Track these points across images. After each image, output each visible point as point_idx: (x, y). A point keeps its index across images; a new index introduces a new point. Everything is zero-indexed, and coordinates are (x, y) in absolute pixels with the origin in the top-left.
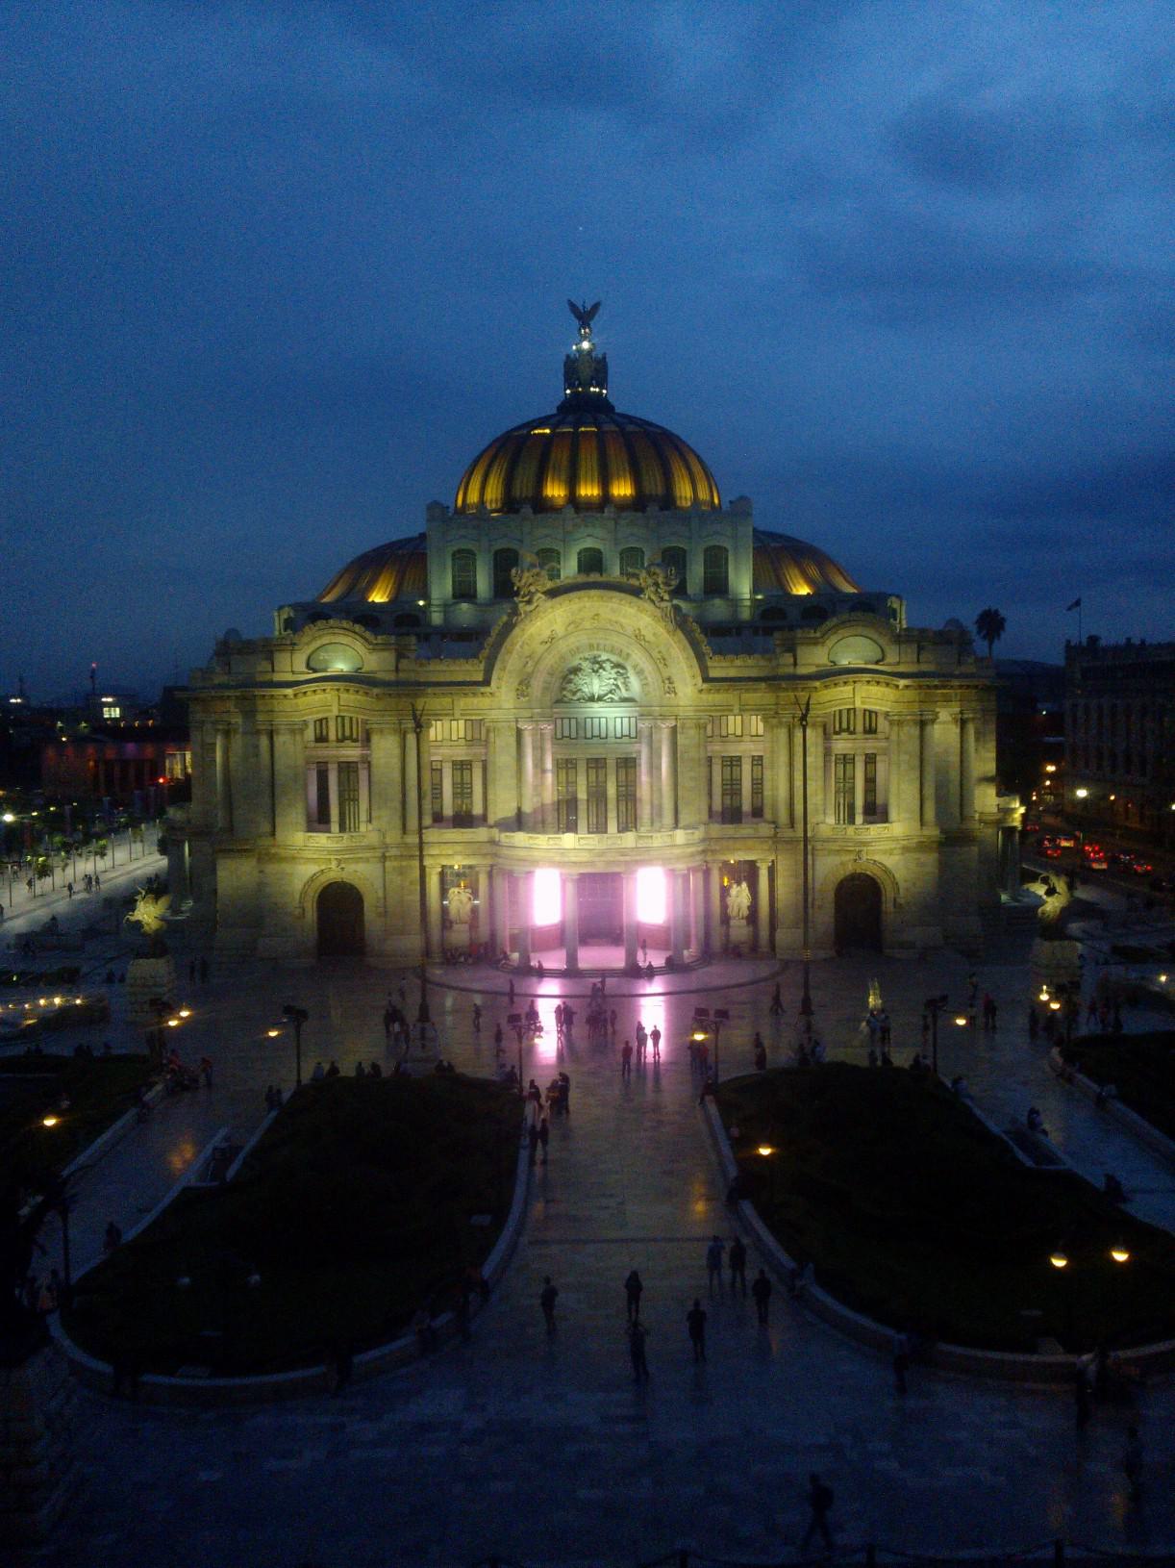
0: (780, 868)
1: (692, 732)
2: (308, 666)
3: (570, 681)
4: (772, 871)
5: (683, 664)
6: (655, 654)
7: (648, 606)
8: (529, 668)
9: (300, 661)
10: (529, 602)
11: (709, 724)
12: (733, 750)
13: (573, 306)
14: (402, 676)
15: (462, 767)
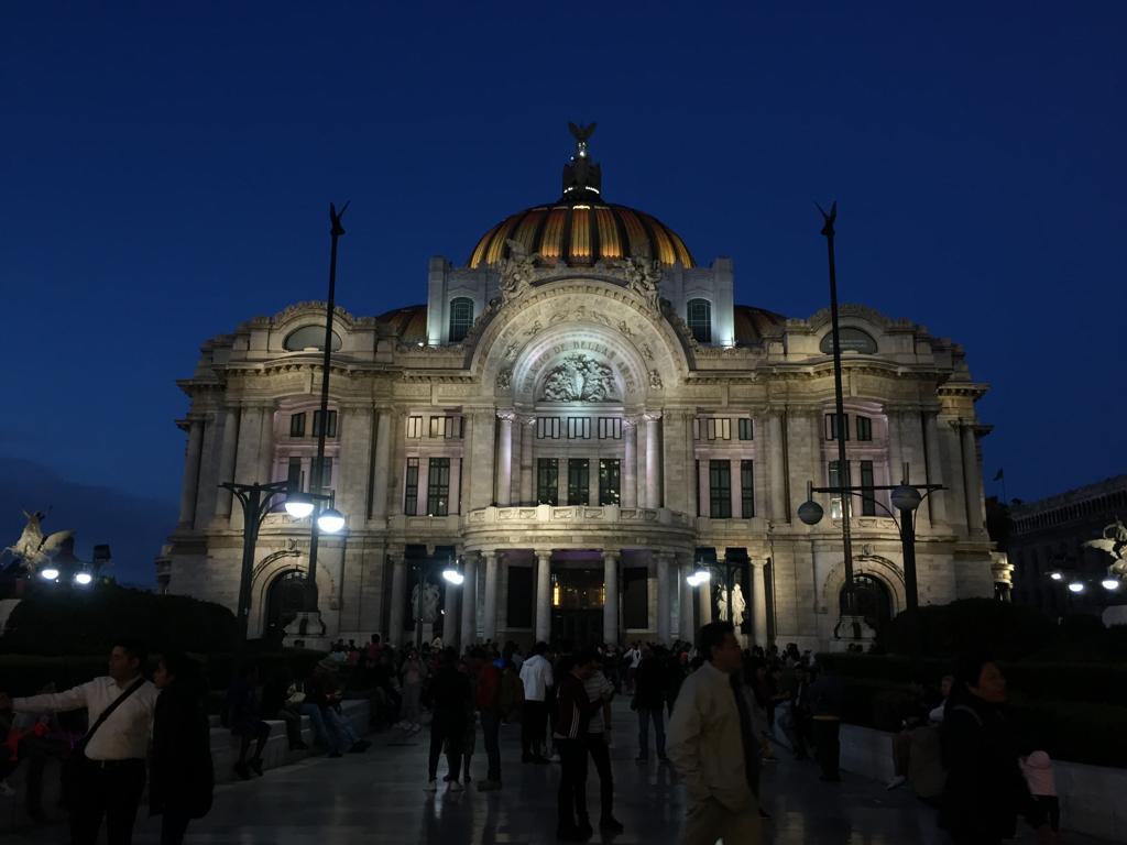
0: (777, 567)
1: (679, 424)
2: (286, 347)
3: (555, 380)
4: (768, 569)
5: (669, 356)
6: (640, 346)
7: (632, 295)
8: (511, 359)
9: (277, 340)
10: (514, 290)
11: (700, 418)
12: (721, 454)
13: (572, 126)
14: (379, 357)
15: (439, 465)
